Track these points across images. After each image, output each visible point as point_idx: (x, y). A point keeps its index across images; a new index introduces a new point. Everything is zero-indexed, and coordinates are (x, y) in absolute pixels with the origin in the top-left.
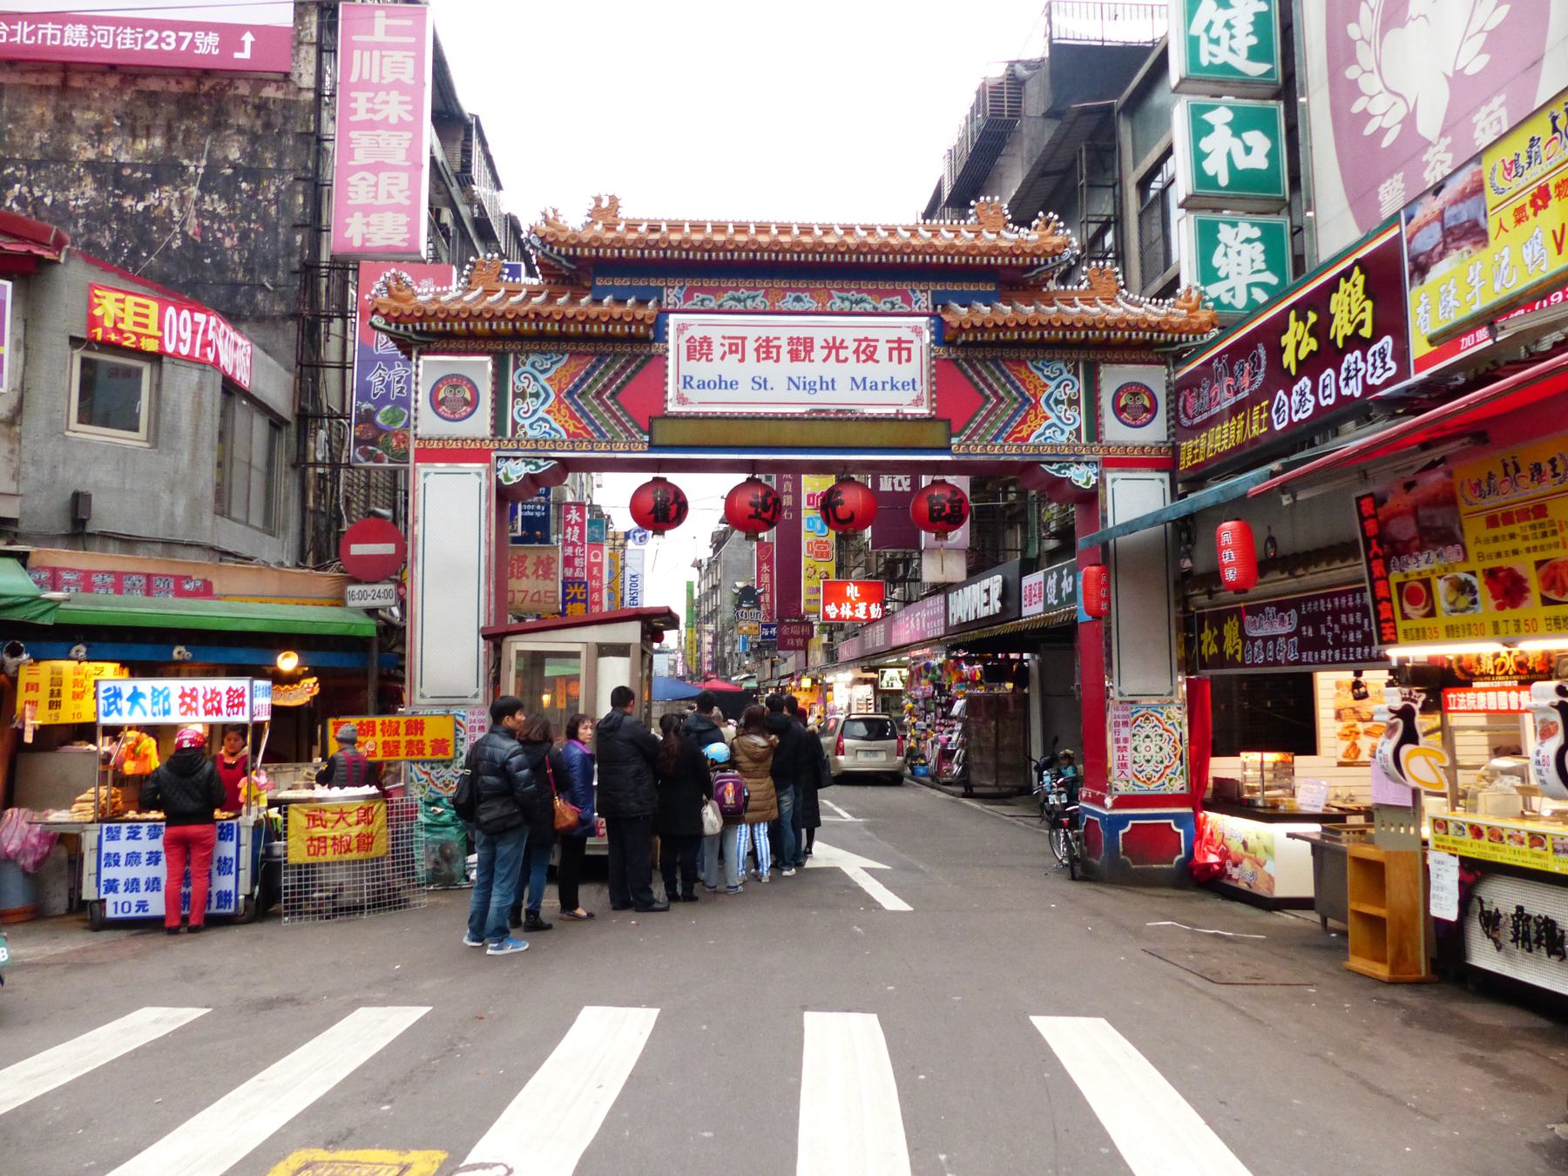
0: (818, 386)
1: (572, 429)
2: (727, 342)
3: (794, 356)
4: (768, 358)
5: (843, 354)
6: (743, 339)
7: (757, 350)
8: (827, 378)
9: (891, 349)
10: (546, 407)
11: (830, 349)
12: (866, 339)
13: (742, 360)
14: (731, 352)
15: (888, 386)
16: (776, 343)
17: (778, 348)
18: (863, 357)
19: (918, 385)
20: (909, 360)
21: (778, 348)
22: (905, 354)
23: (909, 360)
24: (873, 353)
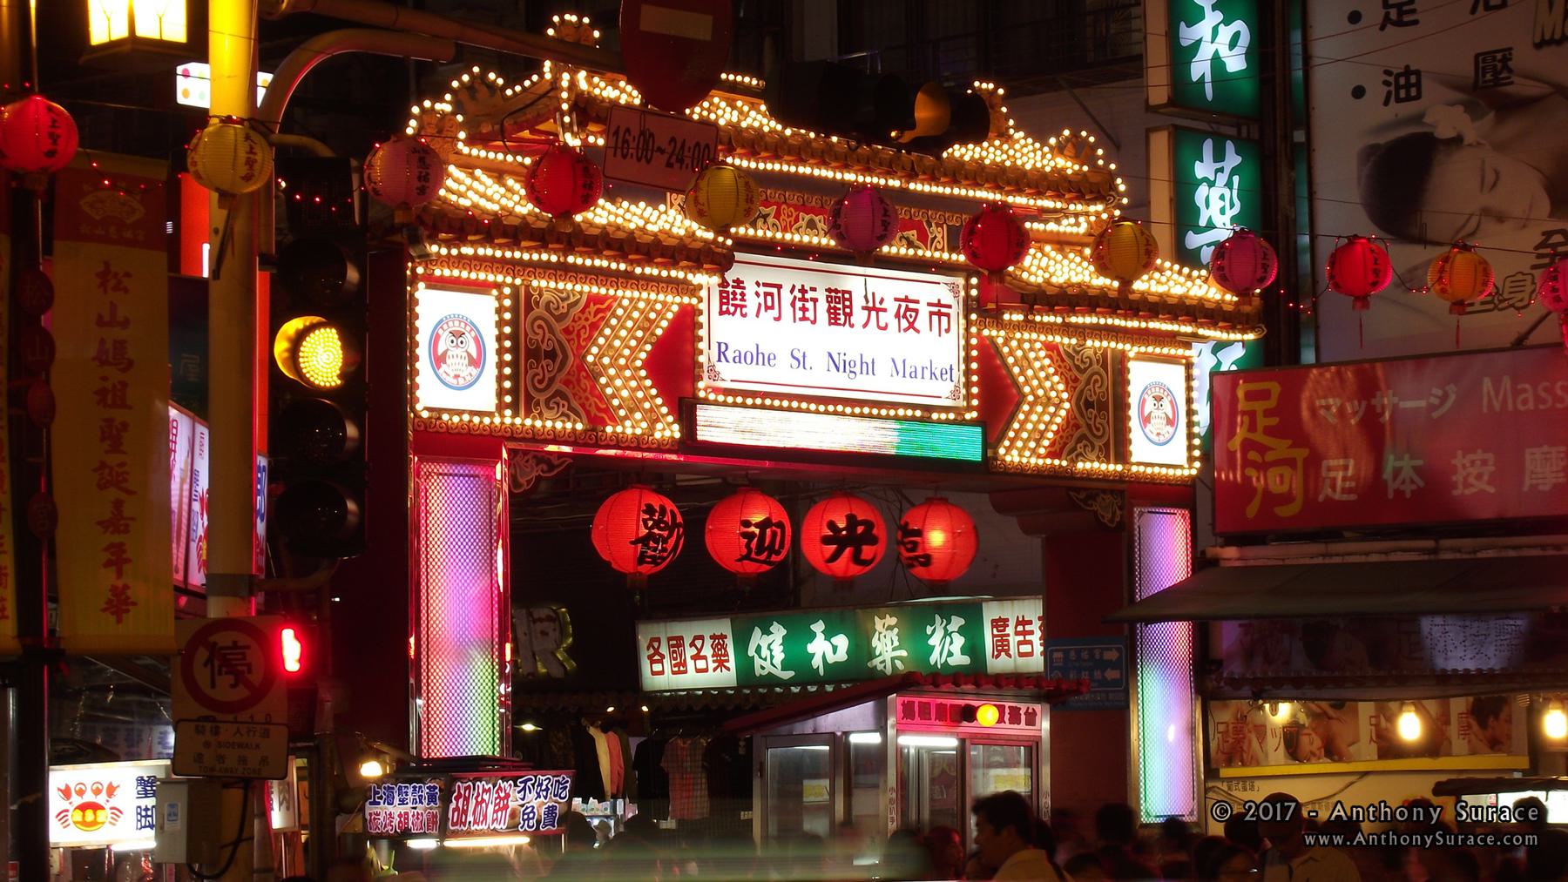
0: (857, 369)
1: (594, 411)
2: (762, 290)
4: (804, 319)
6: (779, 287)
7: (793, 304)
8: (867, 359)
9: (932, 313)
10: (562, 375)
12: (906, 300)
13: (778, 319)
14: (767, 308)
15: (927, 373)
17: (815, 300)
20: (948, 331)
21: (815, 300)
23: (948, 331)
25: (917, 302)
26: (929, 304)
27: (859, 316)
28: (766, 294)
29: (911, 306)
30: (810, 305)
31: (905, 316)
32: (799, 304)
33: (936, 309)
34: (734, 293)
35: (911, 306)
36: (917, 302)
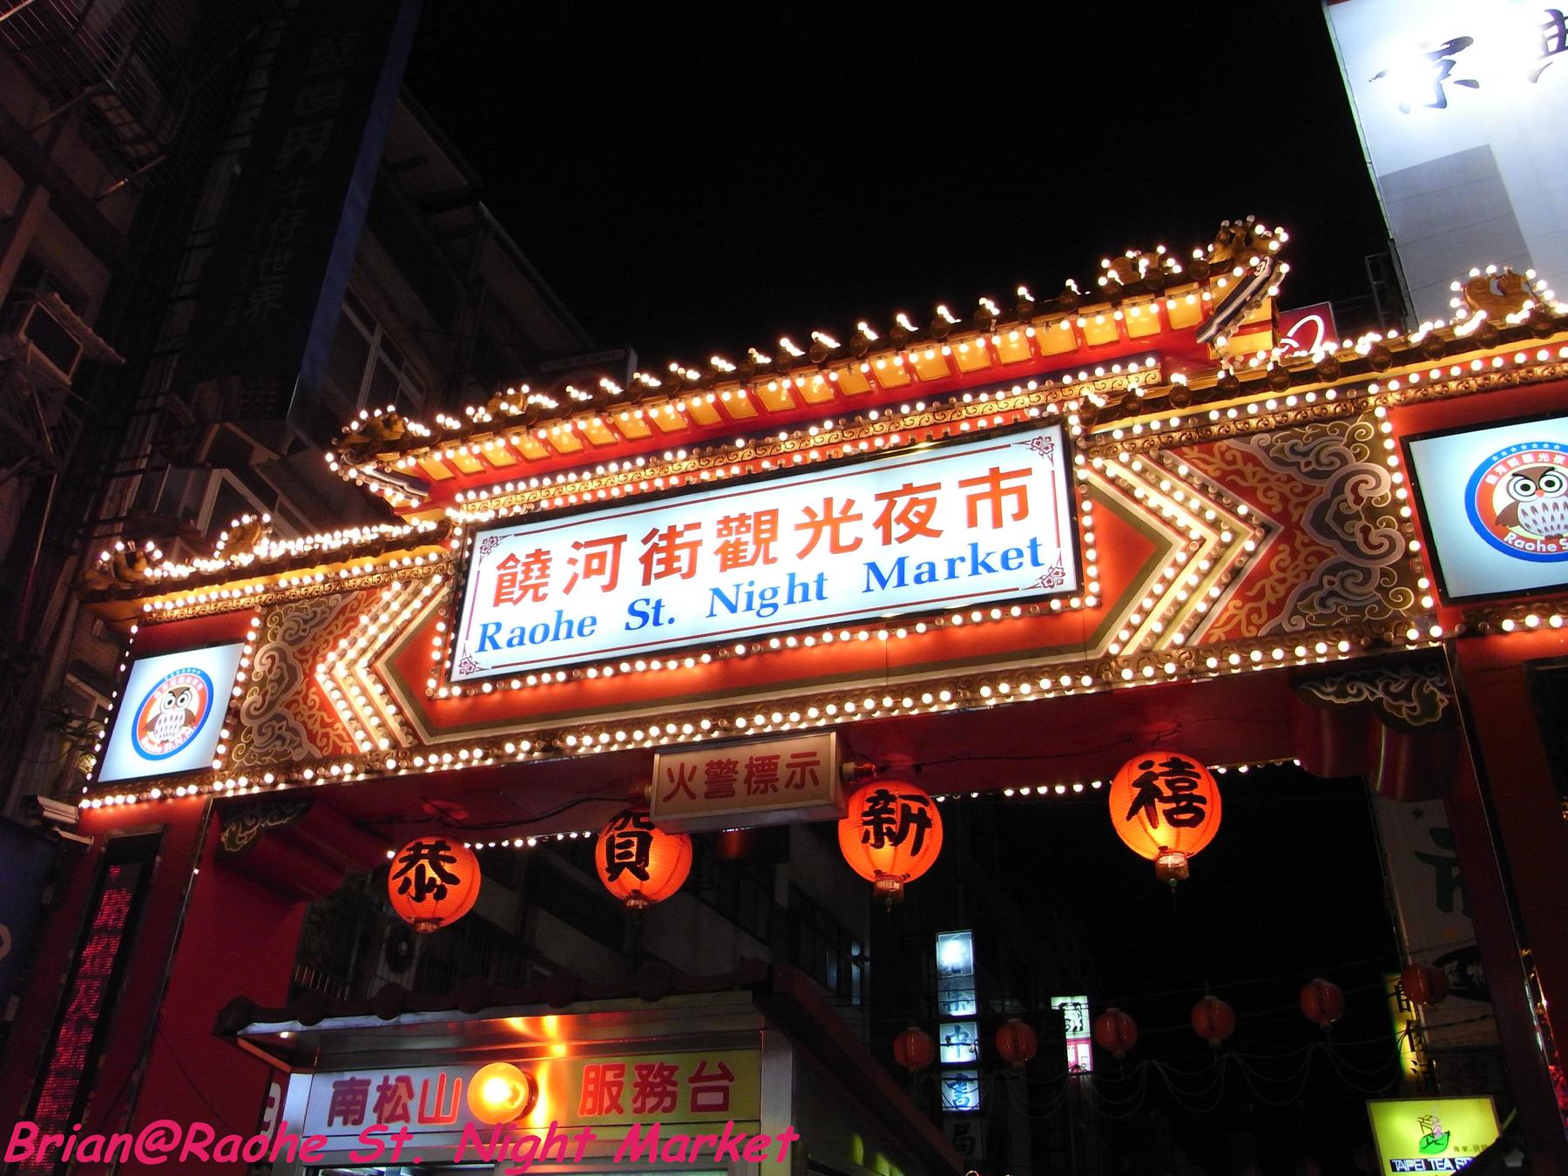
2: (581, 555)
3: (730, 558)
4: (670, 571)
5: (847, 533)
6: (618, 541)
7: (646, 560)
9: (972, 501)
11: (817, 527)
12: (908, 489)
14: (589, 572)
15: (963, 569)
16: (689, 536)
17: (694, 546)
18: (898, 530)
19: (1047, 555)
20: (1022, 513)
22: (1010, 504)
23: (1022, 513)
24: (925, 517)
25: (937, 486)
26: (963, 484)
27: (788, 541)
28: (589, 558)
29: (922, 496)
30: (684, 554)
31: (902, 518)
32: (656, 556)
33: (986, 488)
34: (527, 571)
35: (922, 496)
36: (937, 486)
